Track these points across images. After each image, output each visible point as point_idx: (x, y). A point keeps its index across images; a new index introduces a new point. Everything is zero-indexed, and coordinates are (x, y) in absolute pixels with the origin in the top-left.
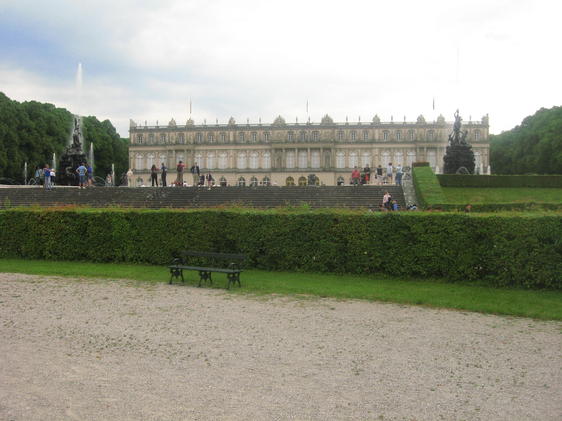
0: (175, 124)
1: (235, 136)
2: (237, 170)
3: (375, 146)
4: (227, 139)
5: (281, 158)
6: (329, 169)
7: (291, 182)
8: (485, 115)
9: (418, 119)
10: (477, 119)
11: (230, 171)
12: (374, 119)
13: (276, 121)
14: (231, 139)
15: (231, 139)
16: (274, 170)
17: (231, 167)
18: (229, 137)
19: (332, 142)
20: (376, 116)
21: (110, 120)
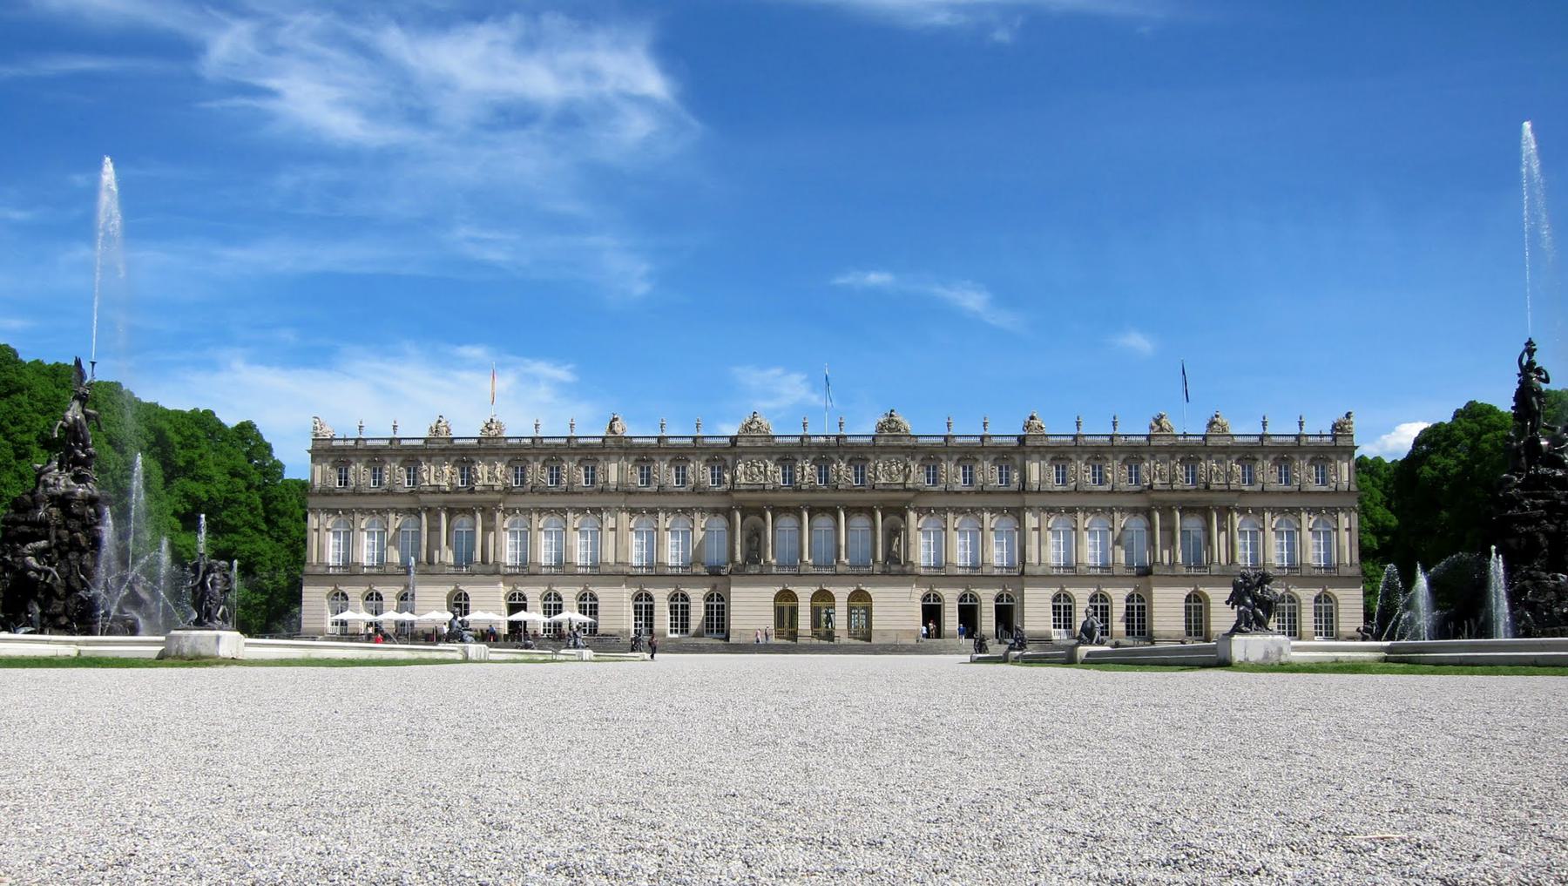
0: (448, 431)
1: (620, 469)
2: (626, 569)
3: (1029, 500)
4: (600, 478)
5: (758, 535)
6: (896, 568)
7: (786, 604)
8: (1340, 416)
9: (1152, 428)
10: (1318, 426)
11: (609, 570)
12: (1028, 426)
13: (747, 428)
14: (613, 478)
15: (613, 478)
16: (740, 572)
17: (611, 560)
18: (606, 472)
19: (909, 490)
20: (1032, 418)
21: (255, 422)
